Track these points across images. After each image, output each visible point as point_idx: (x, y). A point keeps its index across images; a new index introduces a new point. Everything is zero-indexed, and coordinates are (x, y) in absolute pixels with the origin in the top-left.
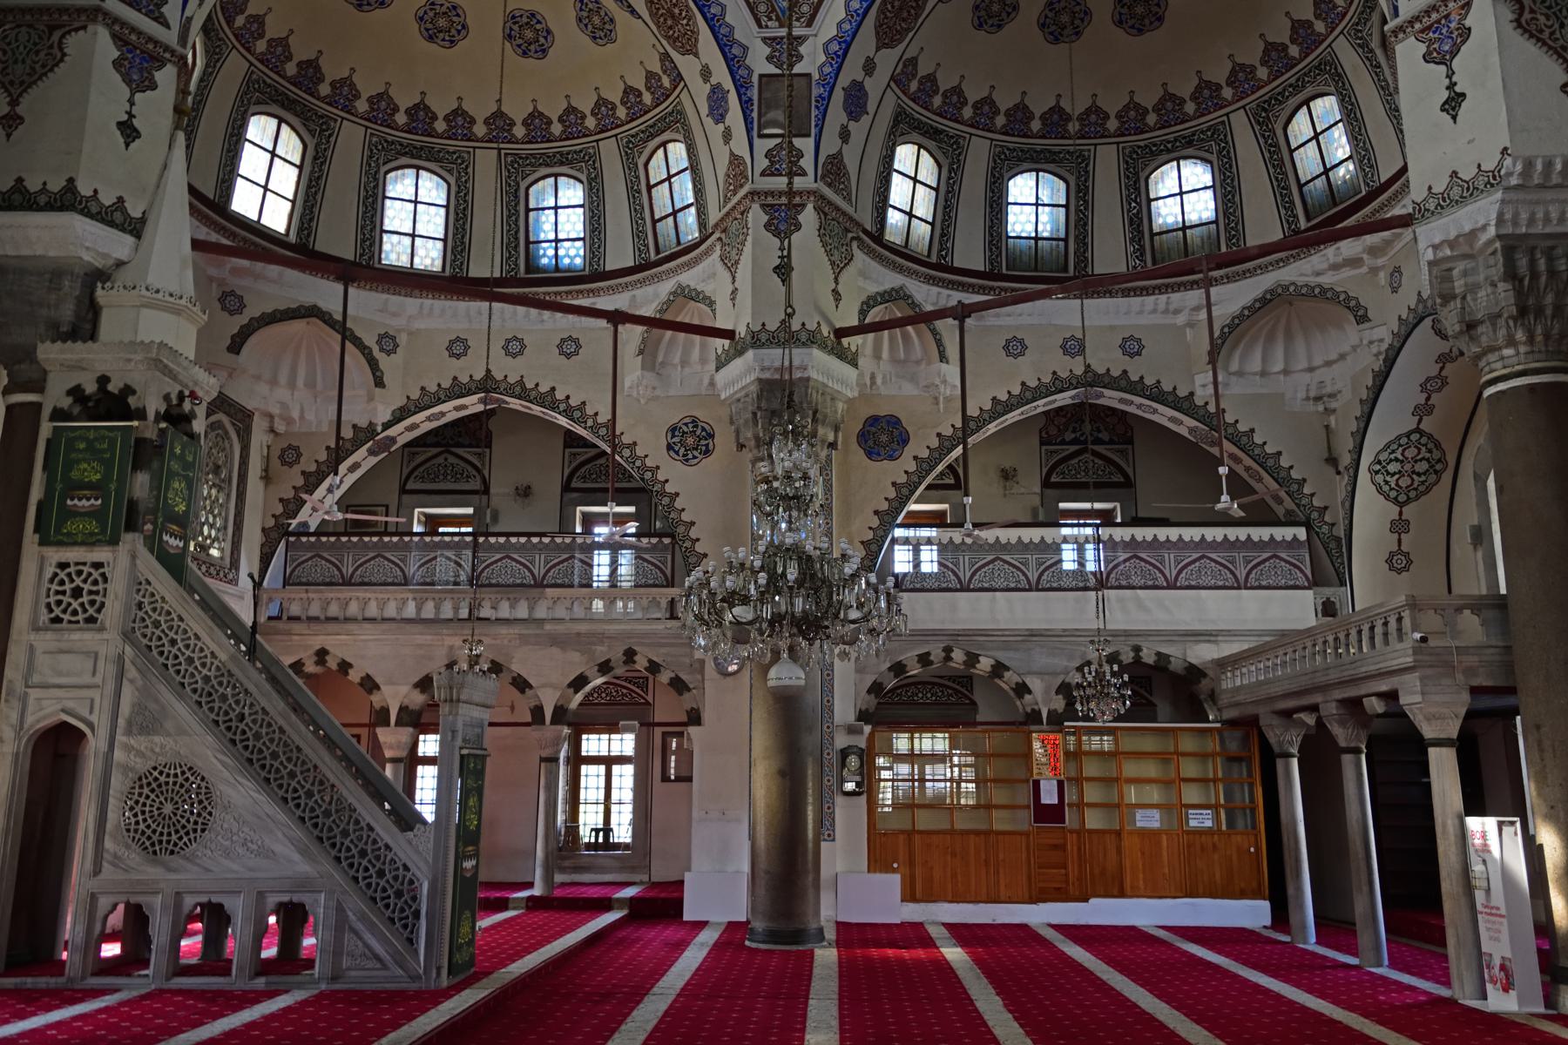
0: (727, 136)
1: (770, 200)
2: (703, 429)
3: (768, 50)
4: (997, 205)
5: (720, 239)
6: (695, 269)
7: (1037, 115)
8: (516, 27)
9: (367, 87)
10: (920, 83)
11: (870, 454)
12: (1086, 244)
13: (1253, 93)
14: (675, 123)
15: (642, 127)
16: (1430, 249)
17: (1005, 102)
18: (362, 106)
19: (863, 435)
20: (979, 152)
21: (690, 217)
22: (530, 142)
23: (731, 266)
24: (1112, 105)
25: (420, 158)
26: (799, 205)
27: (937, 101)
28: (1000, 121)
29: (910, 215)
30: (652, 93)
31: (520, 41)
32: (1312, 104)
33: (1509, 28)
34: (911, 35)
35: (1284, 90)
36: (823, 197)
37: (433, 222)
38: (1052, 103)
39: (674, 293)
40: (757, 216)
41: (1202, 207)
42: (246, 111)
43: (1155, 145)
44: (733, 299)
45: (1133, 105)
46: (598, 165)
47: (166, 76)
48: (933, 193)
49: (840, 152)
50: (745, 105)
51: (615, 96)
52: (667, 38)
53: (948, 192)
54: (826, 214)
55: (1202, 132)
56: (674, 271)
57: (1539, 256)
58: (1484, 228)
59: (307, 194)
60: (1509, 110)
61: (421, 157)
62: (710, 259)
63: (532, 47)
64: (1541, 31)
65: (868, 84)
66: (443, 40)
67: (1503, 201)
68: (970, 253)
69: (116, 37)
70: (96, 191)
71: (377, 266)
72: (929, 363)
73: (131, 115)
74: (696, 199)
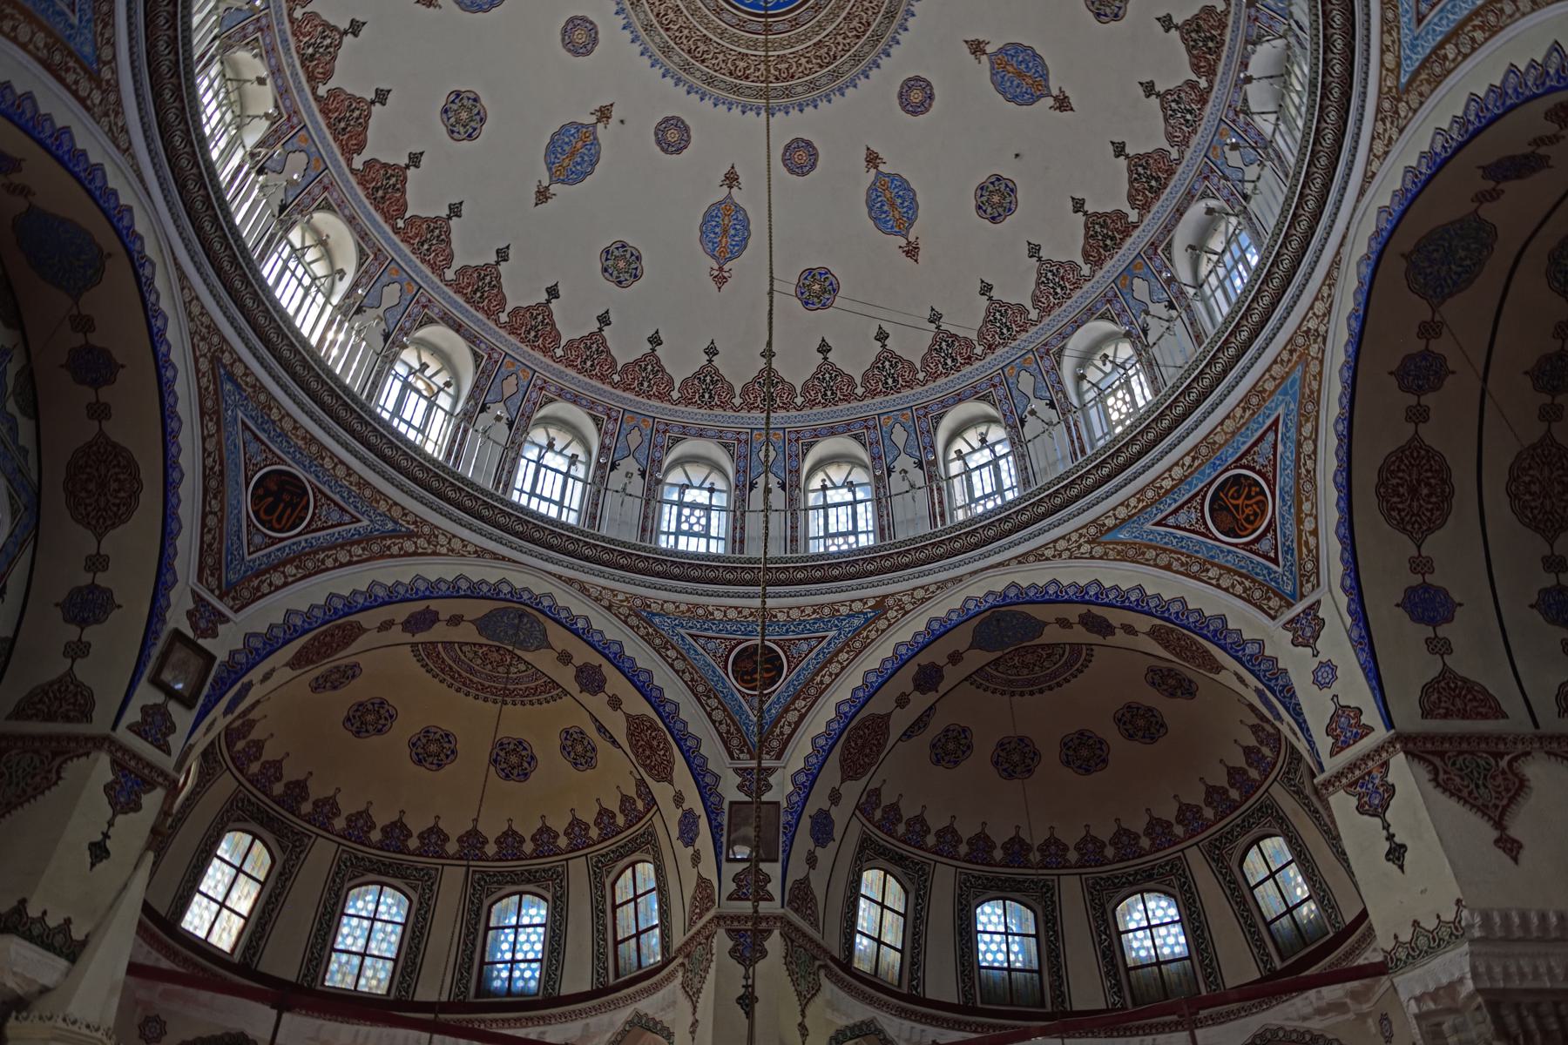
0: (696, 859)
1: (736, 925)
3: (738, 780)
4: (967, 934)
5: (682, 965)
6: (655, 996)
7: (999, 845)
8: (502, 754)
9: (348, 806)
10: (884, 811)
12: (1060, 977)
13: (1203, 831)
14: (646, 845)
15: (613, 847)
16: (1412, 1002)
17: (967, 830)
18: (339, 823)
20: (944, 880)
21: (654, 939)
22: (500, 860)
23: (692, 994)
24: (1071, 837)
25: (386, 874)
26: (765, 931)
27: (901, 829)
28: (963, 849)
29: (879, 941)
30: (626, 815)
31: (505, 766)
32: (1261, 844)
33: (1430, 786)
34: (874, 768)
35: (1232, 830)
36: (789, 923)
37: (387, 942)
38: (1012, 834)
39: (630, 1023)
40: (722, 942)
41: (1173, 942)
42: (223, 828)
43: (1117, 877)
44: (692, 1032)
45: (1089, 839)
46: (565, 883)
47: (152, 801)
48: (901, 919)
49: (807, 878)
50: (715, 830)
51: (589, 817)
52: (644, 766)
53: (916, 919)
54: (792, 941)
55: (1161, 867)
56: (633, 998)
57: (1525, 1013)
58: (1461, 980)
59: (263, 912)
60: (1451, 862)
61: (384, 874)
62: (671, 986)
63: (515, 772)
64: (1460, 790)
65: (834, 813)
66: (432, 763)
67: (1472, 954)
68: (942, 984)
69: (114, 762)
70: (45, 913)
71: (319, 988)
73: (106, 836)
74: (661, 921)
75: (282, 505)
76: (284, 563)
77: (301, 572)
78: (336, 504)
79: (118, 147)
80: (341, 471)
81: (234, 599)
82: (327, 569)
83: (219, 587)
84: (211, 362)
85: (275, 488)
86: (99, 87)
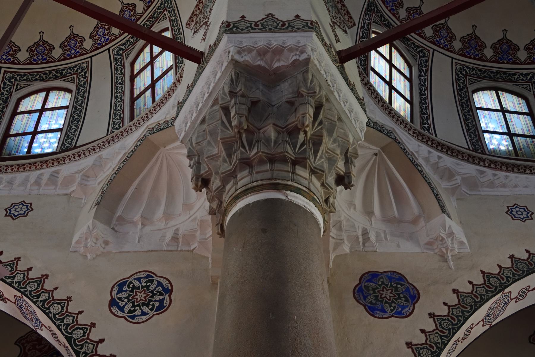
2: (159, 284)
11: (371, 310)
19: (360, 290)
38: (501, 36)
72: (428, 219)
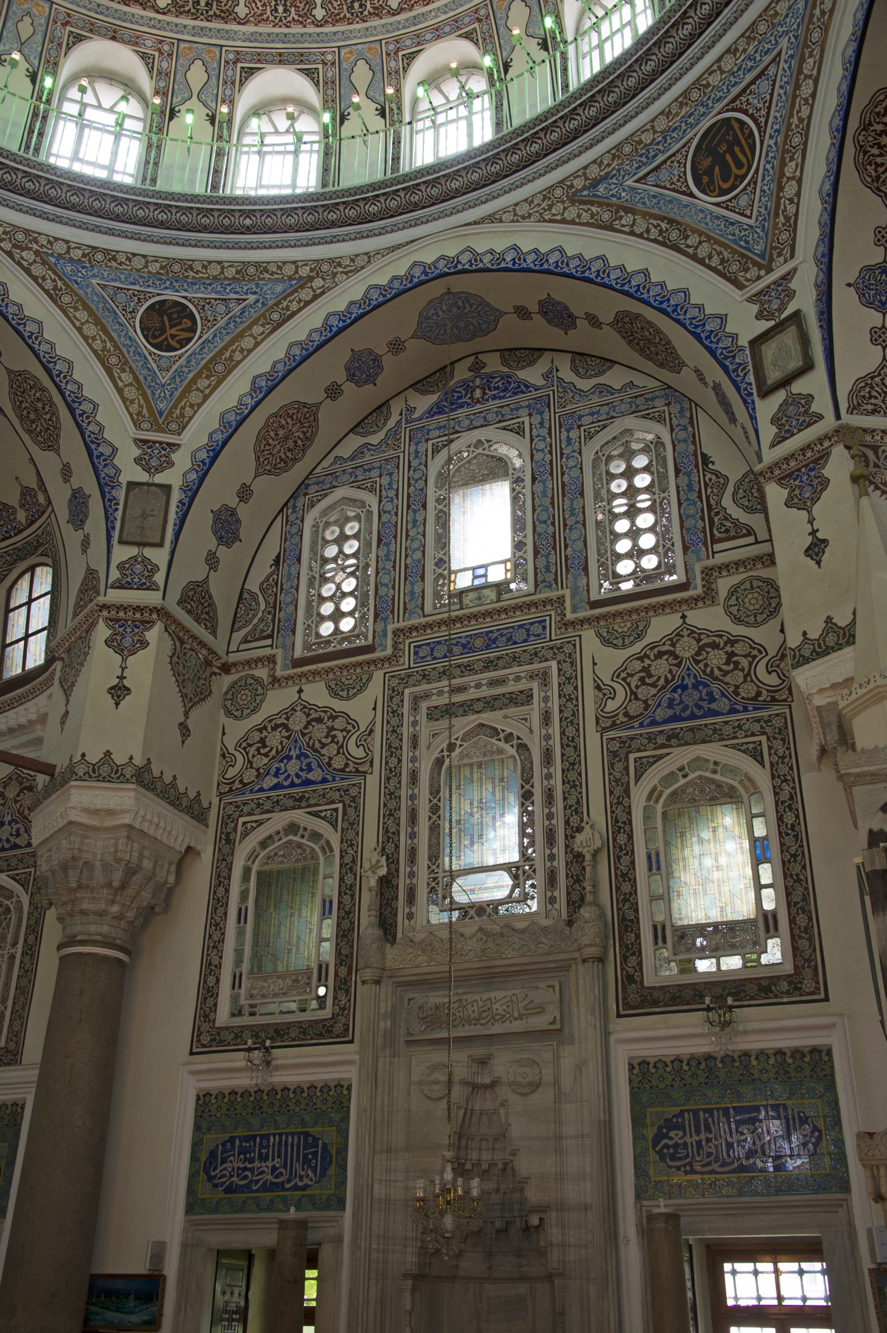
69: (780, 481)
70: (805, 634)
75: (728, 157)
76: (782, 174)
77: (798, 156)
78: (753, 82)
79: (363, 268)
80: (728, 64)
81: (780, 255)
82: (810, 117)
83: (760, 266)
84: (573, 202)
85: (710, 159)
86: (311, 279)
